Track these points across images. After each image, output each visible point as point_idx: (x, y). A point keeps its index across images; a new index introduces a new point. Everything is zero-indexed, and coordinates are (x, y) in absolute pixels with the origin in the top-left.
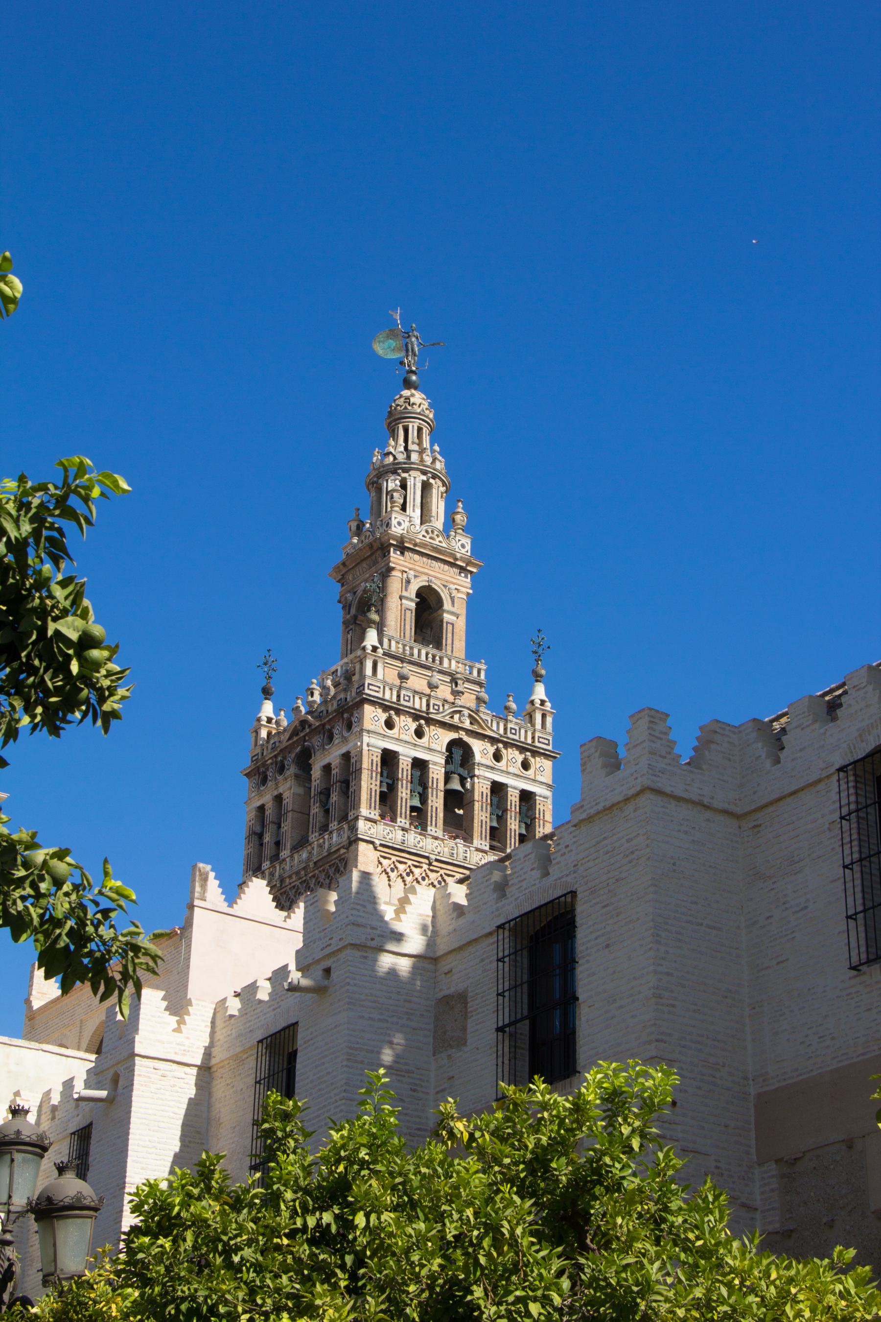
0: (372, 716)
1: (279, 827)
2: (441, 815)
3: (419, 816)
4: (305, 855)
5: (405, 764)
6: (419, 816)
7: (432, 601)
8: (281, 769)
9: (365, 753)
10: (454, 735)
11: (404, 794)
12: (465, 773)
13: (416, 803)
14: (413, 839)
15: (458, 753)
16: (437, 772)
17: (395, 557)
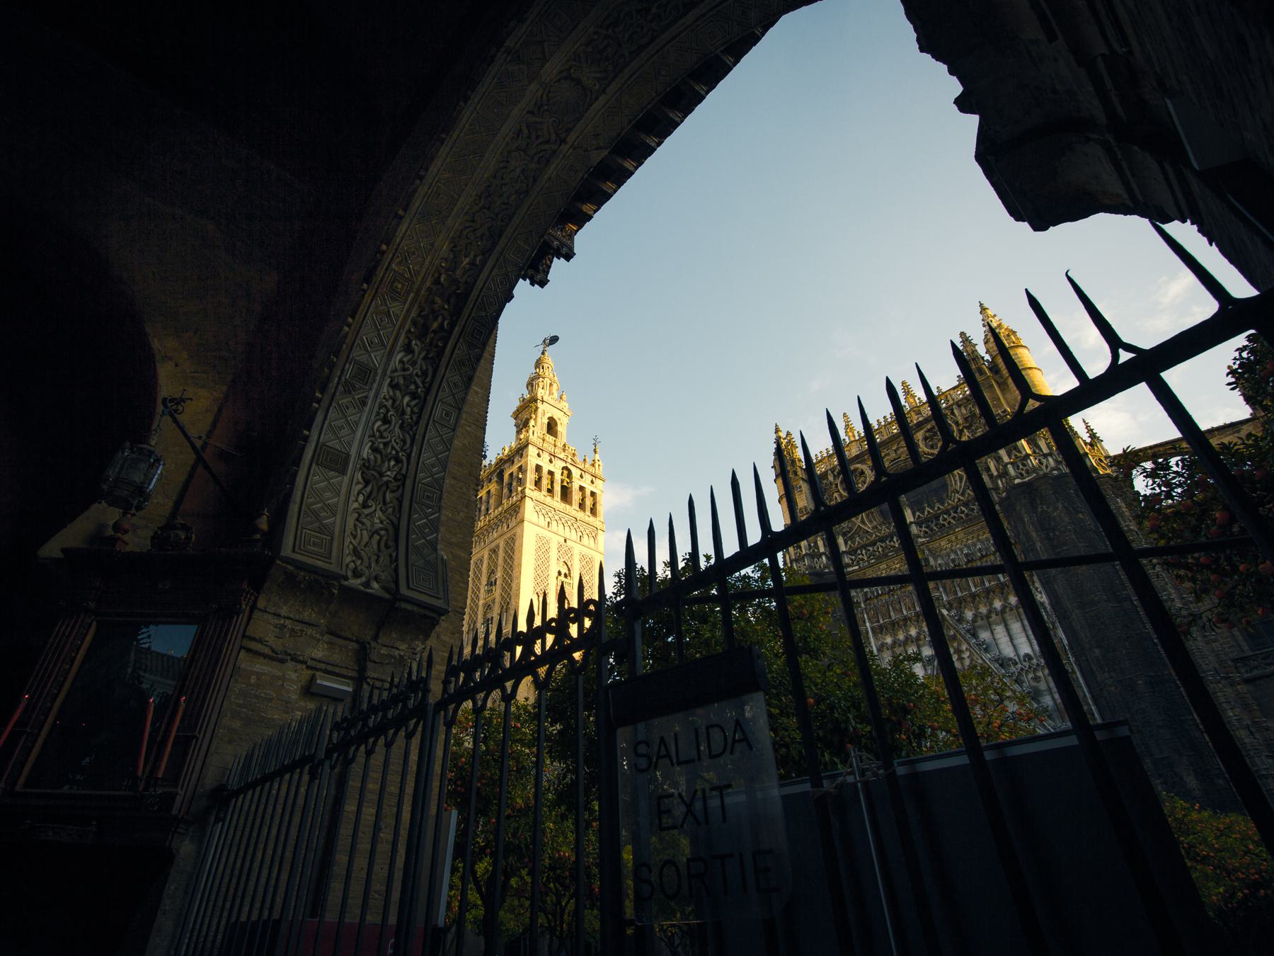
0: (532, 451)
1: (488, 502)
2: (559, 494)
3: (550, 491)
4: (500, 509)
5: (545, 471)
6: (550, 491)
7: (553, 424)
8: (490, 481)
9: (529, 464)
10: (565, 465)
11: (545, 482)
12: (569, 481)
13: (549, 487)
14: (548, 499)
15: (566, 472)
16: (558, 477)
17: (539, 404)
